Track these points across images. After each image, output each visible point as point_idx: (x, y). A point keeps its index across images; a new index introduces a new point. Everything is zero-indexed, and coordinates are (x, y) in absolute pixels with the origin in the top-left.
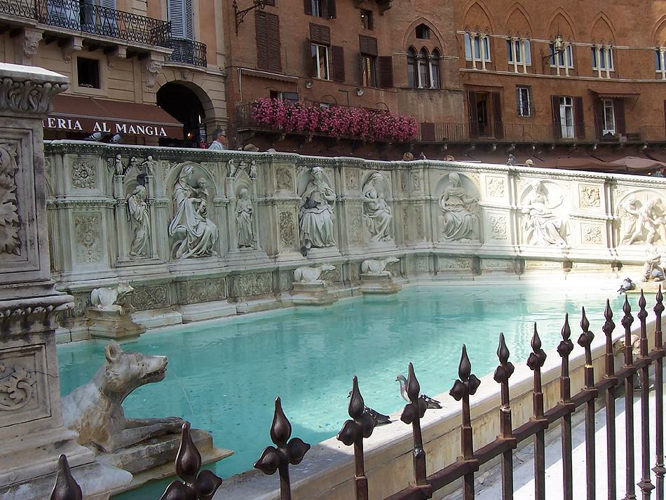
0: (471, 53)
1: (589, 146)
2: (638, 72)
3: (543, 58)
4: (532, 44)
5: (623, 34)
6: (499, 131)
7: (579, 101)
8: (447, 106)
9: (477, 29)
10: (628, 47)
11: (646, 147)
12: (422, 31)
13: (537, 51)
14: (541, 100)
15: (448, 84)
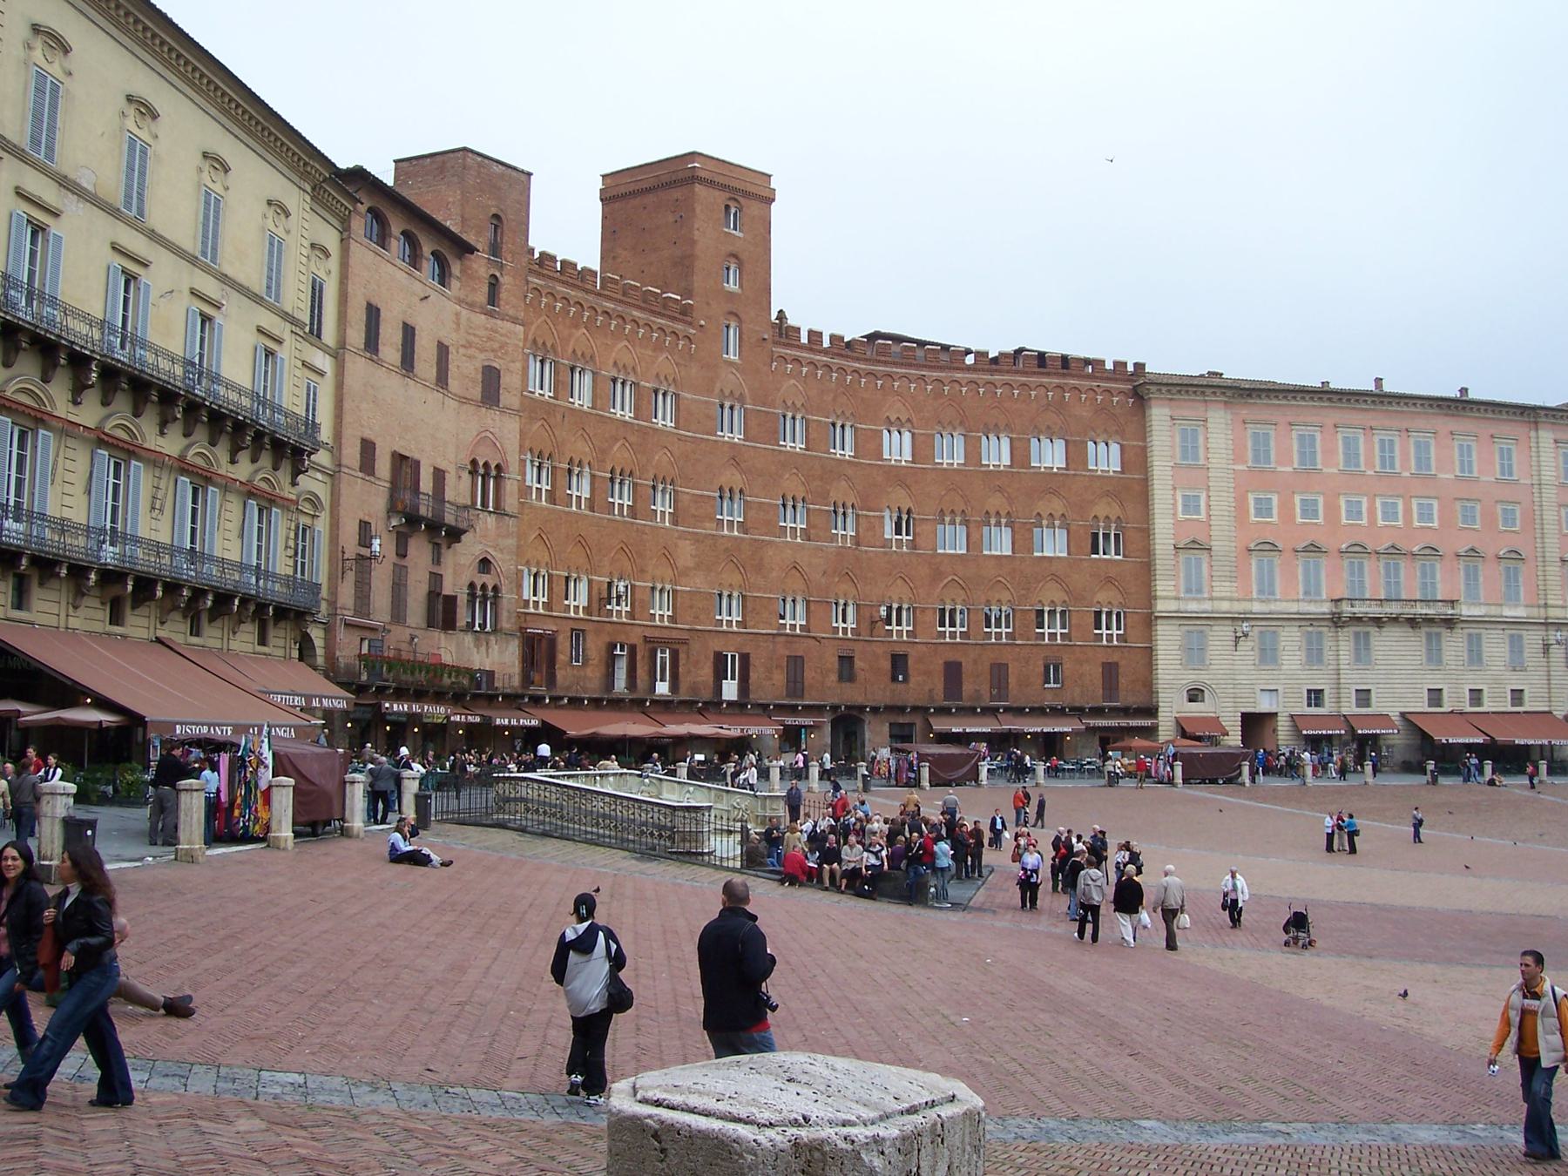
0: (527, 593)
1: (642, 702)
2: (697, 617)
3: (601, 599)
4: (590, 582)
5: (685, 573)
6: (551, 680)
7: (633, 650)
8: (501, 652)
9: (538, 564)
10: (688, 589)
11: (700, 705)
12: (485, 564)
13: (595, 592)
14: (594, 646)
15: (506, 624)
